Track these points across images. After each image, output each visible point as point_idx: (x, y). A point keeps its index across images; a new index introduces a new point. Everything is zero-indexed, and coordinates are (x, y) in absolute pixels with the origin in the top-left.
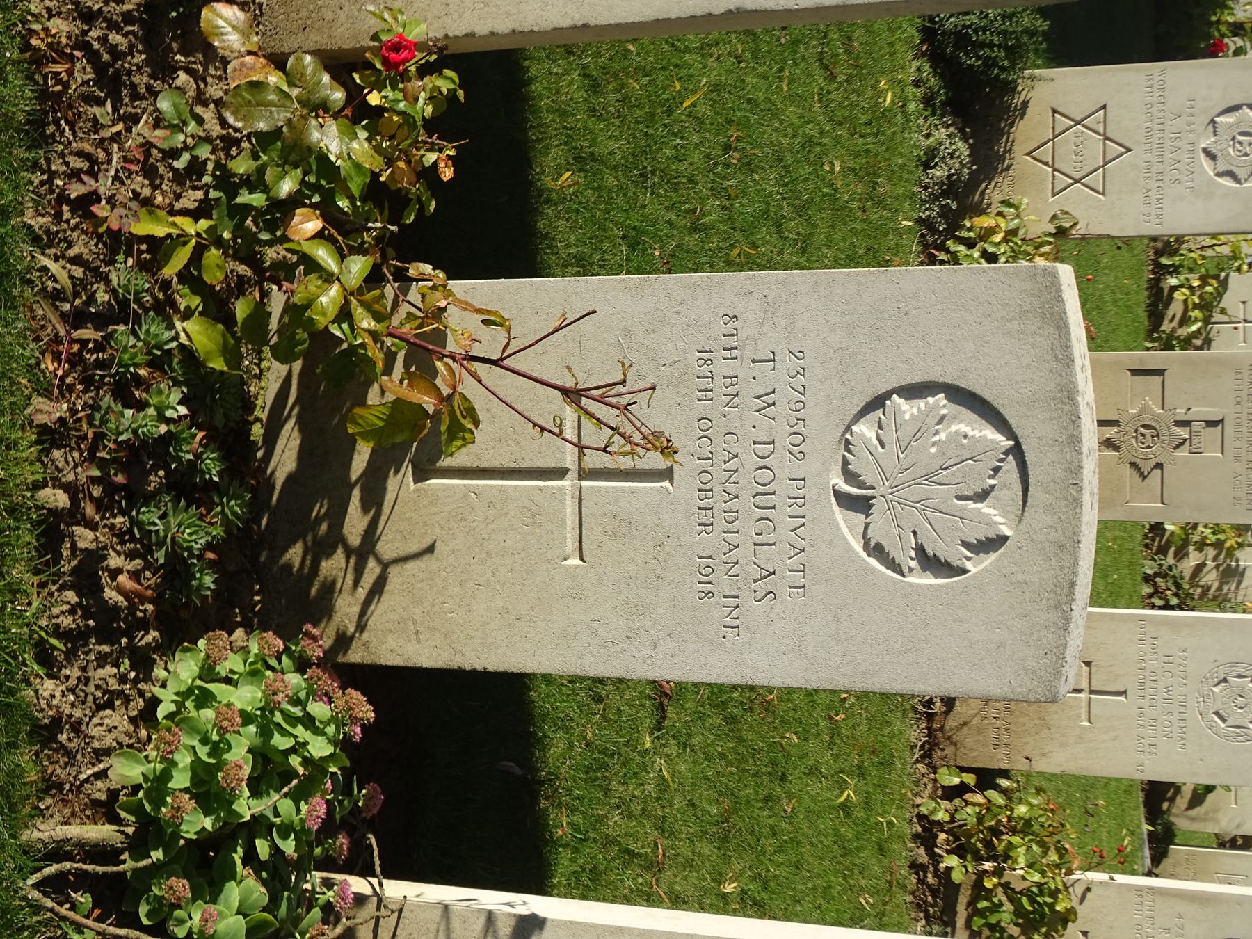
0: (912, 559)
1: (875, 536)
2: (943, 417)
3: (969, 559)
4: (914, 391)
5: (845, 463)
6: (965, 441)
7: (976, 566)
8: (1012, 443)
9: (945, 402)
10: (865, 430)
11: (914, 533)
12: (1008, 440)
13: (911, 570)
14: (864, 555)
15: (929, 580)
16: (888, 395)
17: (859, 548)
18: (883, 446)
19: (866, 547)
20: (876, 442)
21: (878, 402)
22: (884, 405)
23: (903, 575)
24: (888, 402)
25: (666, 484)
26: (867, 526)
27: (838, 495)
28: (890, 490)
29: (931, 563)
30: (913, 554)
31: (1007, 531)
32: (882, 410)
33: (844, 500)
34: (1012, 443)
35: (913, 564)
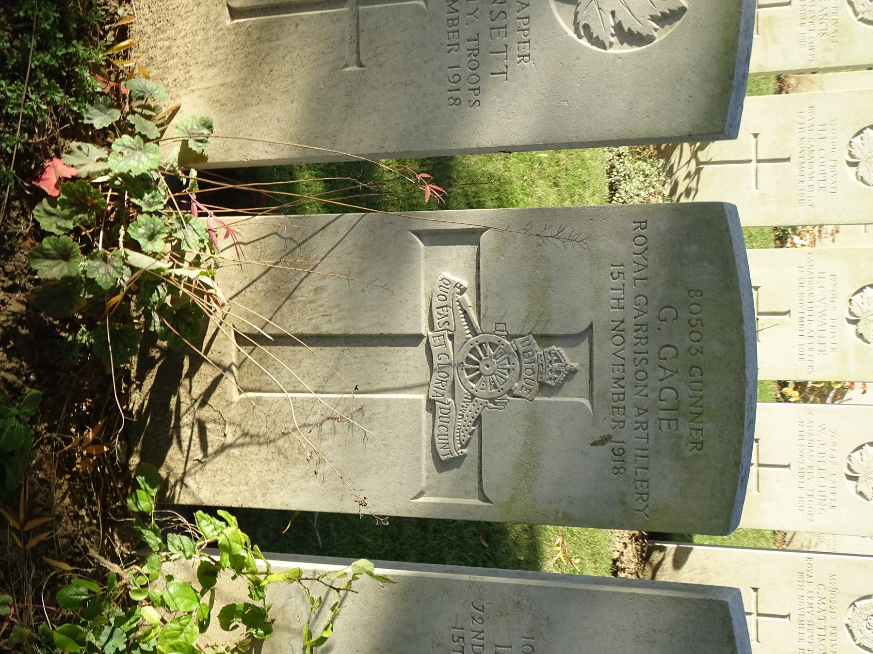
0: (613, 35)
3: (656, 30)
7: (661, 35)
11: (613, 13)
13: (611, 44)
14: (575, 37)
17: (571, 33)
19: (577, 31)
23: (605, 49)
30: (613, 31)
35: (614, 40)
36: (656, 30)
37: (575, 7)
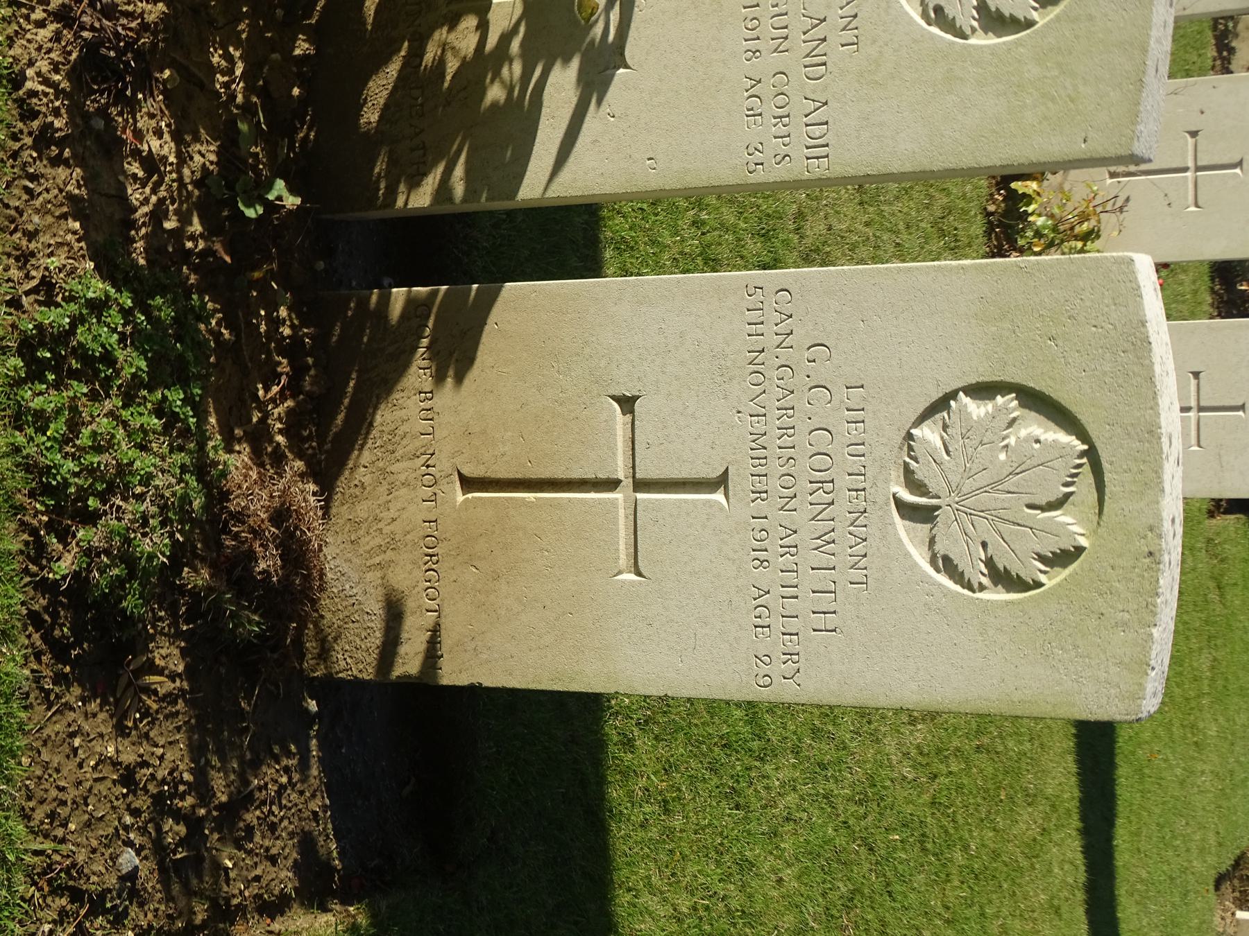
1: (940, 548)
2: (1014, 420)
3: (1041, 571)
4: (982, 391)
5: (908, 472)
6: (1037, 446)
7: (1052, 579)
8: (1086, 447)
9: (1015, 403)
10: (929, 434)
11: (984, 545)
12: (1083, 443)
14: (930, 571)
15: (1000, 596)
16: (953, 395)
18: (948, 452)
19: (933, 562)
20: (939, 444)
21: (942, 404)
22: (948, 407)
23: (974, 592)
24: (952, 403)
25: (719, 497)
26: (932, 542)
27: (900, 505)
28: (957, 499)
29: (1003, 578)
31: (1083, 542)
32: (945, 414)
33: (908, 511)
34: (1086, 447)
35: (985, 581)
36: (1041, 571)
37: (929, 526)
